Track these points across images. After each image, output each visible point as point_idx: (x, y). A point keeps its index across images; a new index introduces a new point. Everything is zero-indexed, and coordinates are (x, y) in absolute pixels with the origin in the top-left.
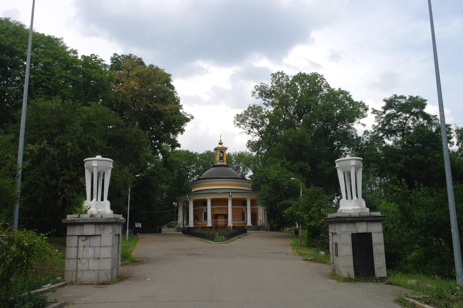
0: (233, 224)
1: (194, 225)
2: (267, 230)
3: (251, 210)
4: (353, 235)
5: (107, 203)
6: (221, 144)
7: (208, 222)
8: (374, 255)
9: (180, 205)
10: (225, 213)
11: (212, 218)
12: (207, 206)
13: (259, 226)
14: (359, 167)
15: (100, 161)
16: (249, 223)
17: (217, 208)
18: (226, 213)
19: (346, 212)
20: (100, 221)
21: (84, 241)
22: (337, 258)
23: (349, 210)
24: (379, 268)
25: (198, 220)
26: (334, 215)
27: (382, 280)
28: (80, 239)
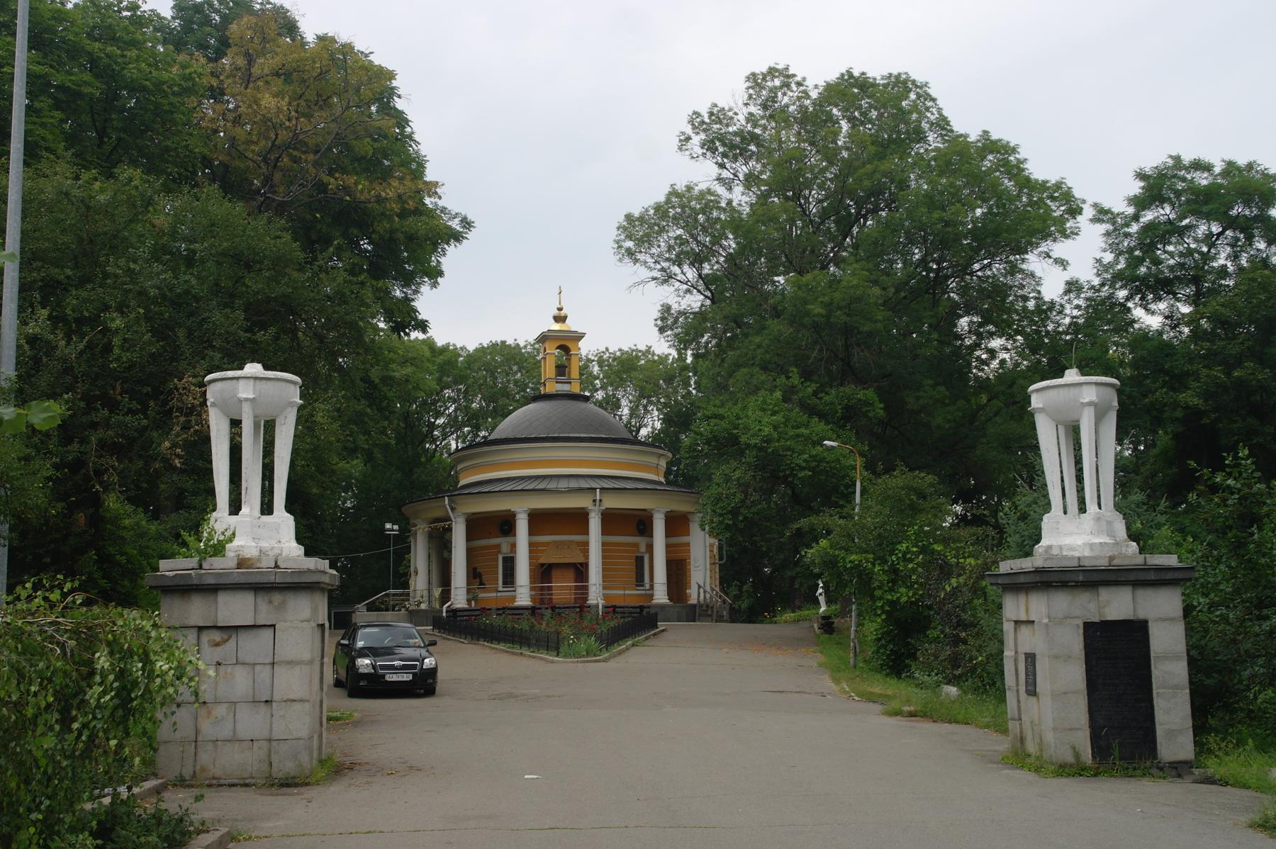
0: (606, 597)
1: (469, 601)
2: (720, 619)
3: (668, 552)
4: (1088, 626)
5: (283, 522)
6: (560, 319)
7: (519, 590)
8: (1154, 692)
10: (579, 559)
12: (515, 535)
13: (694, 606)
14: (1109, 408)
15: (264, 382)
16: (661, 596)
17: (547, 544)
18: (582, 560)
19: (1065, 553)
20: (272, 579)
21: (217, 645)
22: (1033, 700)
23: (1073, 549)
24: (1171, 734)
25: (481, 583)
26: (1026, 564)
27: (1178, 769)
28: (206, 637)
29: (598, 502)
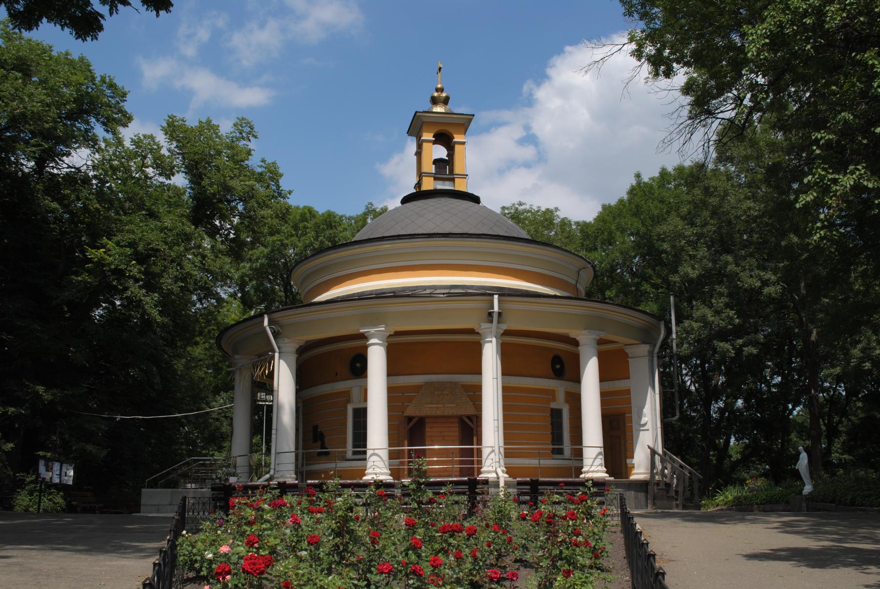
0: (510, 471)
9: (237, 377)
11: (394, 437)
17: (417, 388)
18: (471, 411)
29: (495, 317)
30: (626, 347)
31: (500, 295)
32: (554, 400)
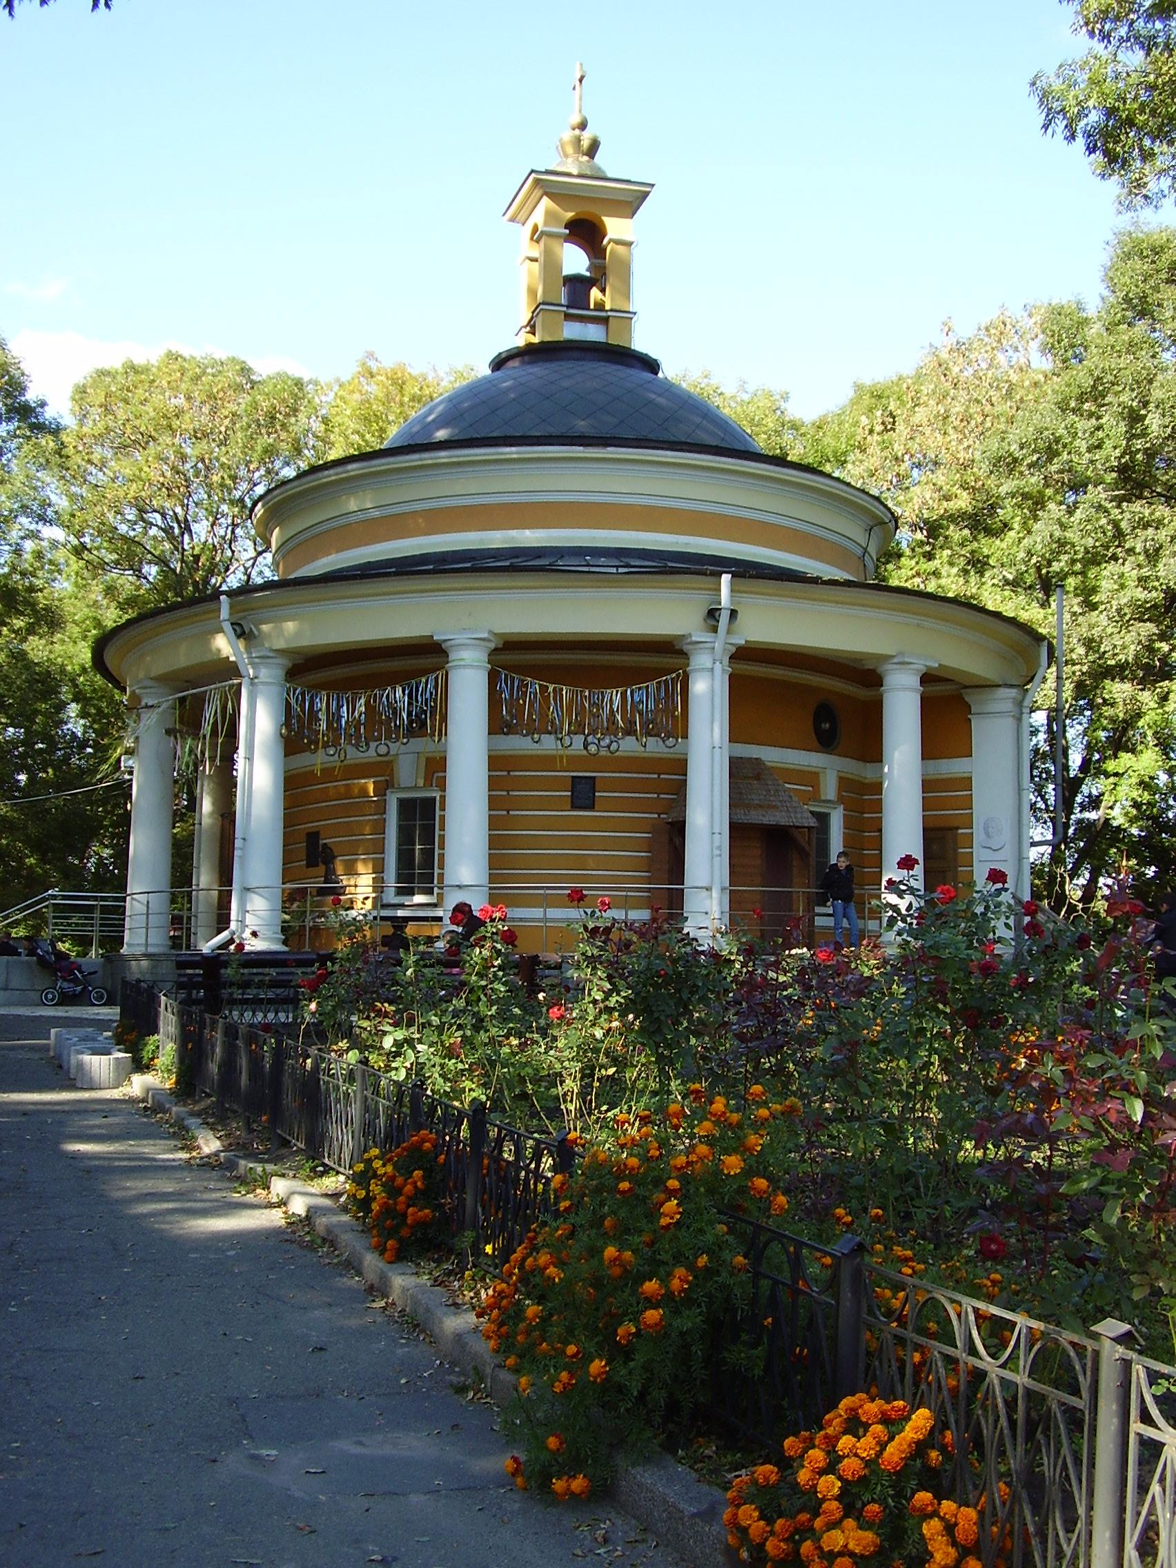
30: (968, 690)
31: (734, 575)
32: (815, 796)
